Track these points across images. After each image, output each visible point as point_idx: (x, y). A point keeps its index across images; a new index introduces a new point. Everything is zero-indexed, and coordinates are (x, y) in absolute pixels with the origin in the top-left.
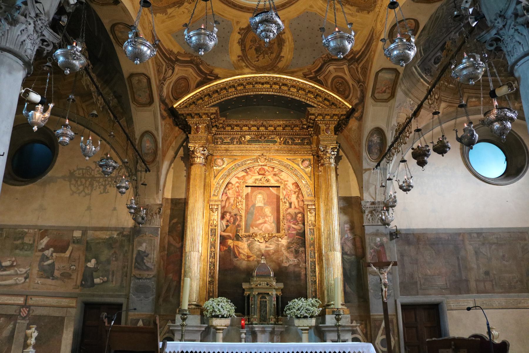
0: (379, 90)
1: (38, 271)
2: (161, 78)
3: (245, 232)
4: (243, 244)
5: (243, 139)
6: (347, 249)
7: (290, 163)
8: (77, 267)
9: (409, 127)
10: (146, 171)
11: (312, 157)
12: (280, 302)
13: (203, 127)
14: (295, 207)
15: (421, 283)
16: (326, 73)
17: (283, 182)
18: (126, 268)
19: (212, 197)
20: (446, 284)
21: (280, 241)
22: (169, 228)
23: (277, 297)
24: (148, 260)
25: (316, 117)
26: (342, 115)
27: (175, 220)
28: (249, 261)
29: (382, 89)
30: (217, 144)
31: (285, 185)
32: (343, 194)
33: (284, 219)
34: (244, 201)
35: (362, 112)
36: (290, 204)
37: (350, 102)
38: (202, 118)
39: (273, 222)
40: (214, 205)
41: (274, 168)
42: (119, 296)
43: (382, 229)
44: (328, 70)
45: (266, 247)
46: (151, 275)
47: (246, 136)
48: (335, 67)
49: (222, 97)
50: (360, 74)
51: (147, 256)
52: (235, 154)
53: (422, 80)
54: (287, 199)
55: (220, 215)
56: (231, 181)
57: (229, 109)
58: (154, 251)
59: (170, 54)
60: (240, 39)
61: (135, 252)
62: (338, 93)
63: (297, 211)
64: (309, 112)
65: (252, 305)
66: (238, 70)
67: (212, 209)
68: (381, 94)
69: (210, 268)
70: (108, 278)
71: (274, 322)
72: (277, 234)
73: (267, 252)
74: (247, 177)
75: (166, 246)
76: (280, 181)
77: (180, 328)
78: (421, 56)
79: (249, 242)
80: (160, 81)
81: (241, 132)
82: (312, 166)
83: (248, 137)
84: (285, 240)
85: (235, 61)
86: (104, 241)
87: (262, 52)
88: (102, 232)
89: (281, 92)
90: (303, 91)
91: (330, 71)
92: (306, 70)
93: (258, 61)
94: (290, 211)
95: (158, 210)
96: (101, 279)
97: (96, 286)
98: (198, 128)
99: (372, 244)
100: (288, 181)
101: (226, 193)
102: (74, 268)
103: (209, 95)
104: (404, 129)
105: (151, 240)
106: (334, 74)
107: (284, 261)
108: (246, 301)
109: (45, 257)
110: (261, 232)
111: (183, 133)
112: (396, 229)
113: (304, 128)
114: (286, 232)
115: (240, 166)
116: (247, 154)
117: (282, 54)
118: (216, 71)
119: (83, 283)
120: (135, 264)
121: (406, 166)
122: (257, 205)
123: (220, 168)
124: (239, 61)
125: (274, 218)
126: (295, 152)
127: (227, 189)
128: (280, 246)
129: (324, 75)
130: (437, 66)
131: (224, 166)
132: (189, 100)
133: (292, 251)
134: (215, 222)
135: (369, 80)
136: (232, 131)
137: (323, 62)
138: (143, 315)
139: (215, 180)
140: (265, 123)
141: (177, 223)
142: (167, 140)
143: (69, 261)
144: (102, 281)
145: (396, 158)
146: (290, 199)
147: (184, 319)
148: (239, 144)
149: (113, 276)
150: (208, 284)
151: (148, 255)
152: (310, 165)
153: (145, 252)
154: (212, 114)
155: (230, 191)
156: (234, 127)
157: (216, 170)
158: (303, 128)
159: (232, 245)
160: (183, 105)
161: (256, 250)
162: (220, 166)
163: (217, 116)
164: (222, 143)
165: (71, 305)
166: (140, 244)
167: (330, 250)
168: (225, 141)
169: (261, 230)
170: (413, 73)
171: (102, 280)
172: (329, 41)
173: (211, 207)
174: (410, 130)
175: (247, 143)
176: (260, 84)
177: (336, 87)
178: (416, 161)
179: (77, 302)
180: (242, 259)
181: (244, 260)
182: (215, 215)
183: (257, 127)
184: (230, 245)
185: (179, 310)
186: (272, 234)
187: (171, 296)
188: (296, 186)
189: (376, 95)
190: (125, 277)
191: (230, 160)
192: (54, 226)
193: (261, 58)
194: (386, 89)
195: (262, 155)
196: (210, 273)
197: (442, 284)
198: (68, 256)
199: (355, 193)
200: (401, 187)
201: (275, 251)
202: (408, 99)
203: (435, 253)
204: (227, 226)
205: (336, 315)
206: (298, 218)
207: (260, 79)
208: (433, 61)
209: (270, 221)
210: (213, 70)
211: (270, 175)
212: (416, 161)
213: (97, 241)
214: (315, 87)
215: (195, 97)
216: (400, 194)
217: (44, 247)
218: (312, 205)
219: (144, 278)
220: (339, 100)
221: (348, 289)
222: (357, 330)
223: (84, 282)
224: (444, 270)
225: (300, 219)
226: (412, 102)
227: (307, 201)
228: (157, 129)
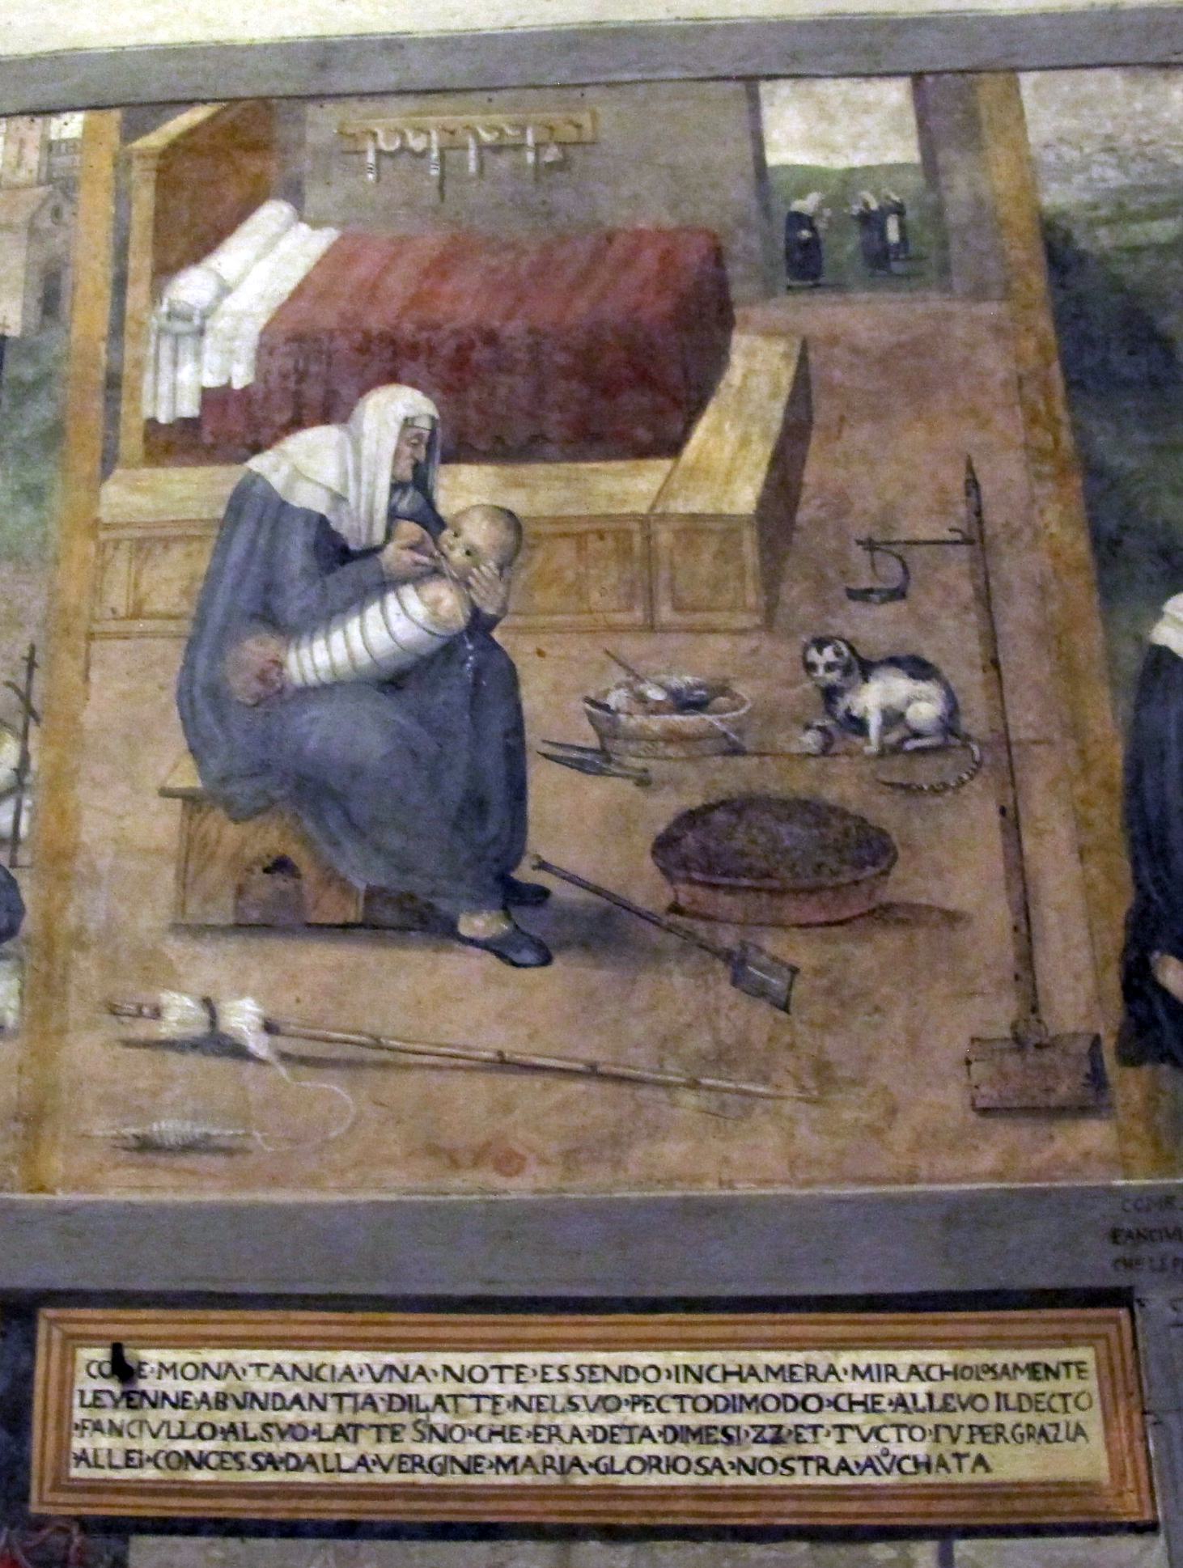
1: (191, 800)
8: (969, 680)
102: (926, 709)
109: (297, 553)
143: (771, 580)
192: (393, 46)
198: (745, 497)
217: (241, 376)
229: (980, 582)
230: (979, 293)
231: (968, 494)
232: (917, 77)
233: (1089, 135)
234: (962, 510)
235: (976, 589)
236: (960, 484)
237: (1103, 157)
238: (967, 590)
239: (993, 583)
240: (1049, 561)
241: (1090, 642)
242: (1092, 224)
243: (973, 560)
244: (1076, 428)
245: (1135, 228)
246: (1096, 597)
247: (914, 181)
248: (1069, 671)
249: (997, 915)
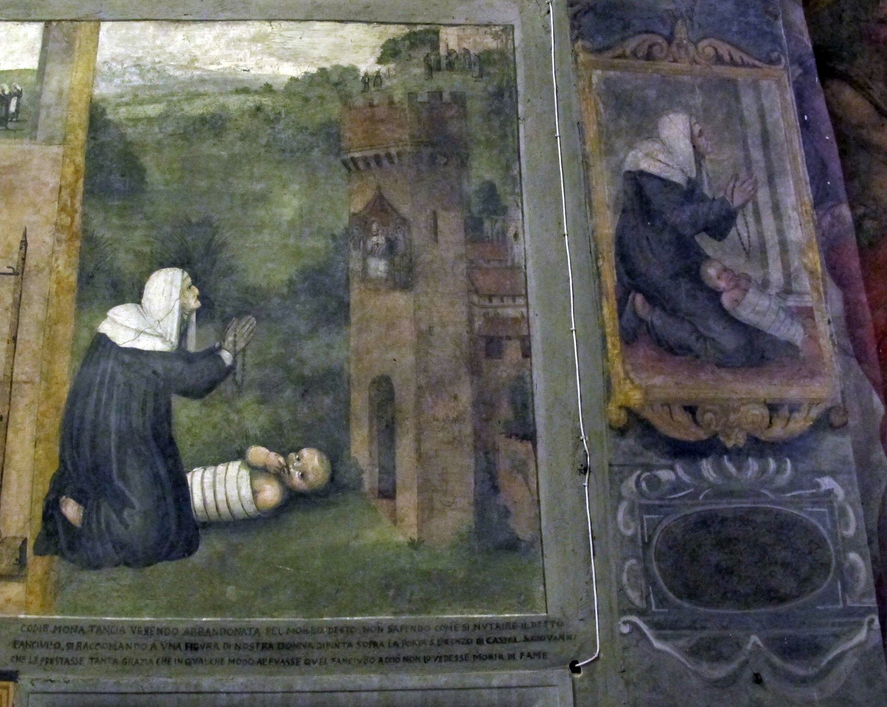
18: (512, 351)
24: (739, 263)
46: (794, 408)
58: (771, 181)
86: (267, 101)
96: (256, 471)
119: (72, 510)
144: (271, 493)
171: (280, 475)
190: (521, 448)
213: (197, 108)
223: (79, 501)
229: (17, 296)
230: (49, 141)
231: (21, 248)
232: (48, 22)
233: (129, 57)
234: (16, 257)
235: (14, 299)
236: (17, 245)
237: (133, 69)
238: (9, 300)
239: (23, 296)
240: (55, 286)
241: (65, 331)
242: (118, 105)
243: (16, 284)
244: (84, 215)
245: (140, 108)
246: (74, 306)
247: (31, 79)
248: (51, 344)
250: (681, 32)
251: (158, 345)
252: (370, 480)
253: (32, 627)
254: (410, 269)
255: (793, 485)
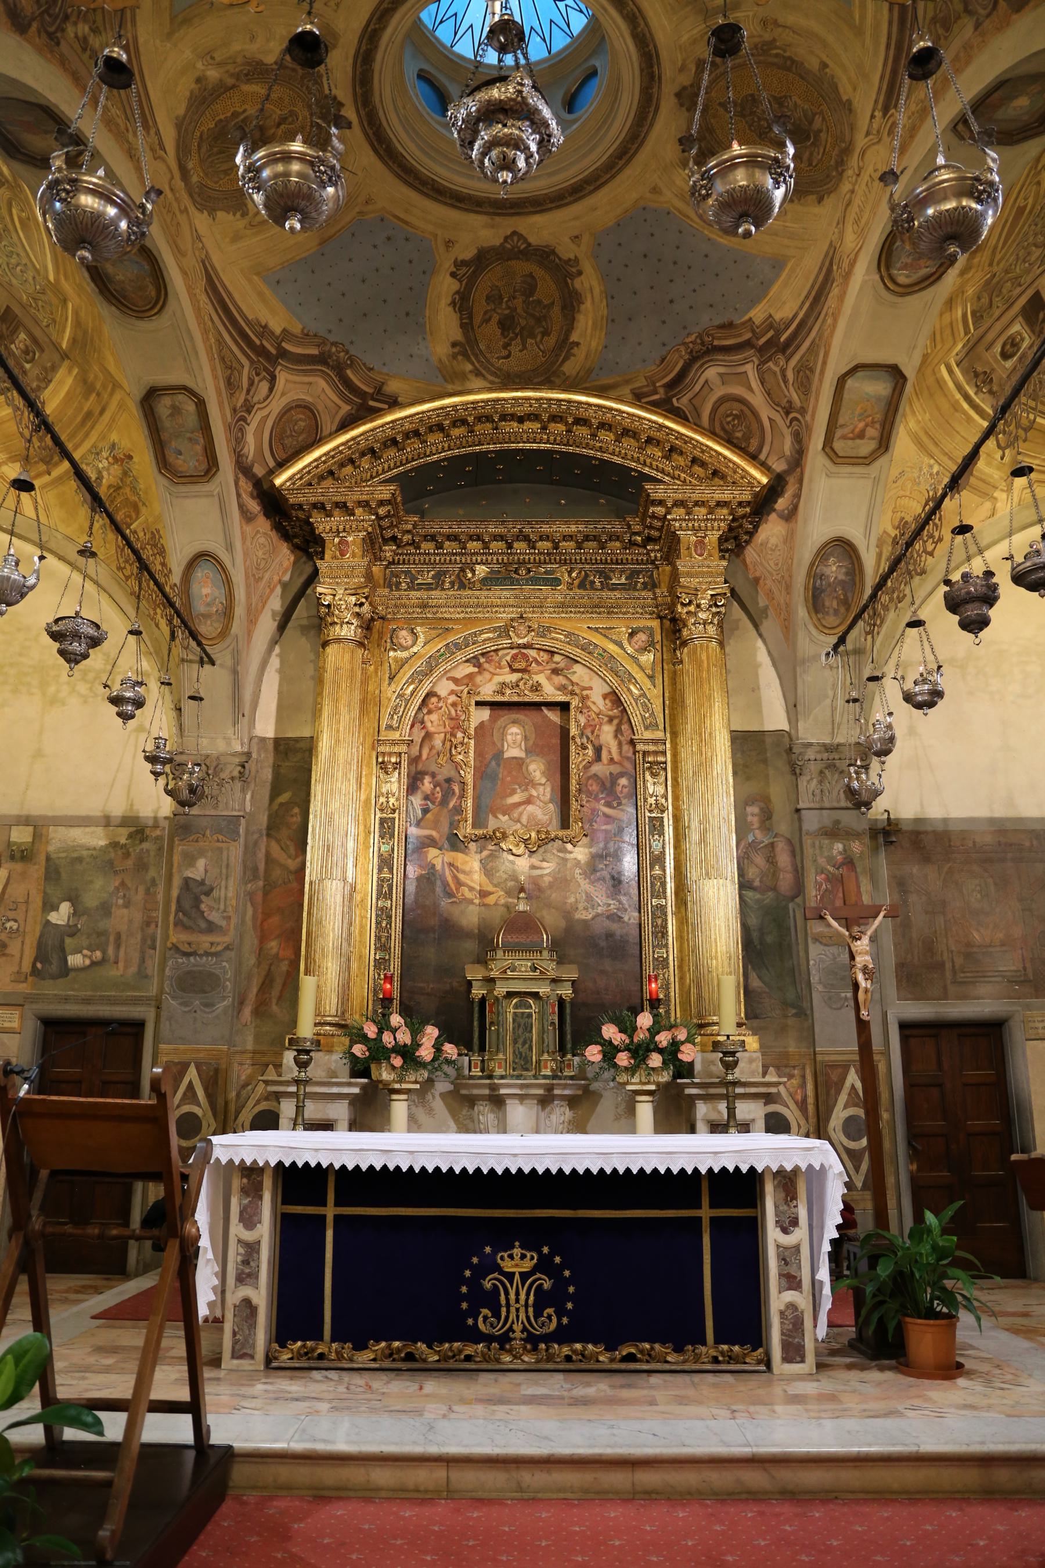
0: (846, 430)
2: (239, 405)
3: (474, 826)
4: (467, 858)
5: (470, 575)
6: (752, 873)
7: (597, 639)
8: (22, 923)
9: (935, 524)
10: (202, 662)
11: (655, 624)
12: (568, 1018)
13: (359, 541)
14: (612, 759)
15: (953, 966)
16: (697, 388)
17: (577, 691)
18: (153, 926)
19: (382, 733)
20: (1025, 969)
21: (571, 852)
22: (270, 817)
23: (561, 1002)
24: (212, 903)
25: (668, 513)
26: (740, 504)
27: (284, 797)
28: (485, 905)
29: (856, 427)
30: (398, 589)
31: (584, 699)
32: (741, 725)
33: (580, 791)
34: (472, 742)
35: (798, 496)
36: (598, 750)
37: (764, 467)
38: (354, 515)
39: (551, 801)
40: (390, 754)
41: (552, 653)
42: (136, 1001)
43: (849, 819)
44: (702, 381)
45: (533, 867)
46: (218, 944)
47: (478, 567)
48: (722, 370)
49: (410, 457)
50: (791, 389)
51: (208, 893)
52: (446, 616)
53: (966, 406)
54: (588, 738)
55: (405, 780)
56: (435, 690)
57: (431, 493)
59: (261, 336)
60: (457, 292)
61: (177, 882)
62: (730, 442)
63: (615, 769)
64: (648, 495)
65: (492, 1024)
66: (453, 383)
67: (383, 766)
68: (850, 442)
69: (378, 923)
70: (104, 952)
71: (552, 1070)
72: (561, 833)
73: (535, 881)
74: (479, 679)
75: (262, 866)
76: (570, 688)
77: (293, 1089)
78: (966, 334)
79: (485, 853)
80: (235, 410)
81: (461, 554)
82: (658, 647)
83: (481, 570)
84: (581, 849)
85: (444, 359)
86: (94, 852)
87: (517, 331)
88: (87, 830)
89: (571, 442)
90: (634, 438)
91: (706, 382)
92: (641, 382)
93: (508, 357)
94: (596, 768)
95: (239, 768)
96: (85, 956)
97: (72, 974)
98: (343, 542)
99: (822, 861)
100: (591, 688)
101: (422, 722)
102: (15, 926)
103: (372, 451)
104: (918, 533)
105: (220, 849)
106: (719, 392)
107: (581, 906)
108: (476, 1015)
110: (519, 825)
111: (304, 559)
112: (889, 819)
113: (635, 544)
114: (587, 826)
115: (460, 649)
116: (479, 615)
117: (574, 337)
118: (393, 386)
119: (39, 965)
120: (176, 915)
121: (925, 638)
122: (506, 755)
123: (405, 654)
124: (454, 356)
125: (552, 790)
126: (610, 611)
127: (425, 711)
128: (569, 865)
129: (690, 395)
130: (1009, 364)
131: (415, 649)
132: (317, 467)
133: (604, 879)
134: (392, 800)
135: (817, 400)
136: (437, 554)
137: (687, 357)
138: (199, 1051)
139: (393, 685)
140: (527, 530)
141: (286, 806)
142: (261, 579)
144: (88, 962)
145: (895, 619)
146: (598, 736)
147: (302, 1065)
148: (459, 589)
149: (118, 946)
150: (372, 968)
151: (211, 890)
152: (652, 643)
153: (202, 883)
154: (381, 503)
155: (434, 717)
156: (442, 543)
157: (396, 659)
158: (633, 544)
159: (438, 864)
160: (301, 478)
161: (505, 876)
162: (407, 649)
163: (396, 509)
164: (411, 588)
165: (7, 1025)
166: (190, 860)
167: (707, 874)
168: (419, 581)
169: (519, 821)
170: (940, 383)
171: (90, 957)
172: (710, 179)
173: (380, 760)
174: (936, 534)
175: (478, 585)
176: (512, 420)
177: (723, 429)
178: (957, 618)
179: (21, 1017)
180: (465, 899)
181: (471, 902)
182: (393, 780)
183: (506, 541)
184: (434, 862)
185: (290, 1040)
186: (547, 832)
187: (274, 1001)
188: (613, 702)
189: (838, 445)
190: (152, 952)
191: (434, 633)
193: (515, 348)
194: (867, 425)
195: (522, 617)
196: (378, 938)
197: (1013, 968)
199: (775, 719)
200: (908, 698)
201: (556, 879)
202: (927, 460)
203: (996, 884)
204: (425, 811)
205: (725, 1054)
206: (619, 788)
207: (513, 406)
208: (997, 348)
209: (542, 798)
210: (383, 383)
211: (541, 672)
212: (957, 618)
213: (75, 855)
214: (667, 427)
215: (333, 457)
216: (904, 717)
218: (656, 753)
219: (201, 952)
220: (734, 463)
221: (755, 983)
222: (779, 1094)
224: (1017, 932)
225: (626, 790)
226: (936, 469)
227: (647, 742)
228: (230, 547)
249: (18, 956)
250: (208, 832)
251: (62, 923)
252: (112, 958)
253: (28, 994)
254: (129, 902)
255: (215, 964)
